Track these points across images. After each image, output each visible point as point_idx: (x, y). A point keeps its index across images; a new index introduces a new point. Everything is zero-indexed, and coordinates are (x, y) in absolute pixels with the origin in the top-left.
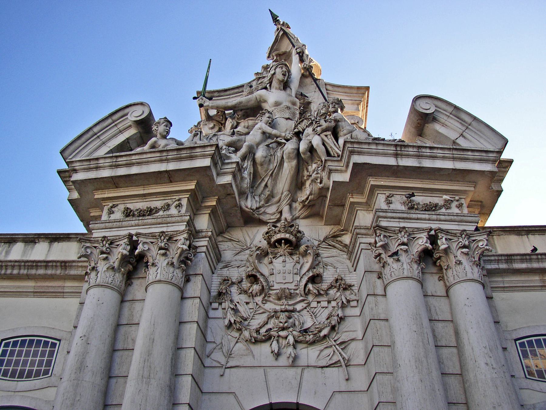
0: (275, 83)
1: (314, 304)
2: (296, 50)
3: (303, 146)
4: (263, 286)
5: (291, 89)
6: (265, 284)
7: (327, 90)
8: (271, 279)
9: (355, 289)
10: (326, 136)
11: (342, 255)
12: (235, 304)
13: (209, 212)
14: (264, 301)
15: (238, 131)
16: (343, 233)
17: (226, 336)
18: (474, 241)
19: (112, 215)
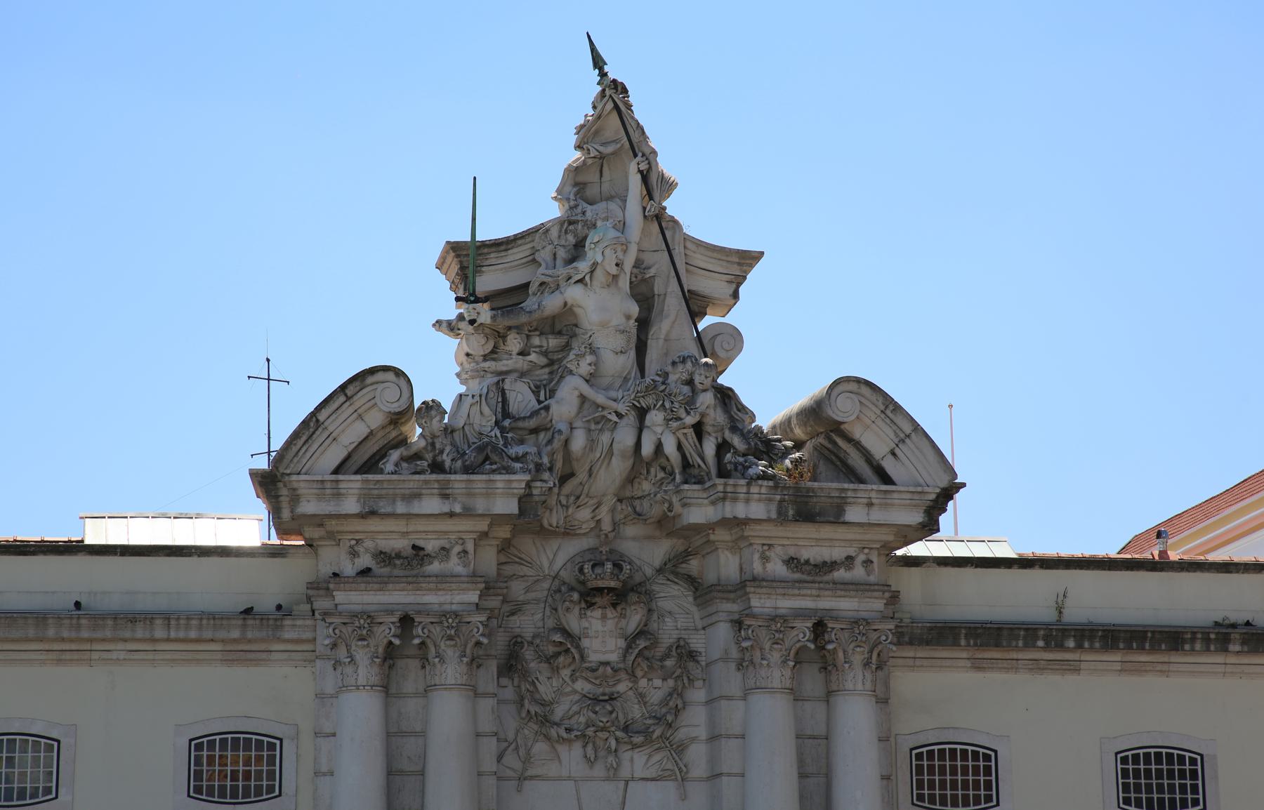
0: (599, 273)
1: (643, 683)
2: (638, 164)
3: (647, 449)
4: (574, 658)
5: (626, 273)
6: (577, 656)
7: (685, 247)
8: (585, 643)
9: (704, 654)
10: (685, 434)
11: (686, 596)
12: (533, 681)
13: (497, 543)
14: (573, 678)
15: (531, 362)
16: (691, 557)
17: (521, 730)
18: (875, 630)
19: (356, 560)
